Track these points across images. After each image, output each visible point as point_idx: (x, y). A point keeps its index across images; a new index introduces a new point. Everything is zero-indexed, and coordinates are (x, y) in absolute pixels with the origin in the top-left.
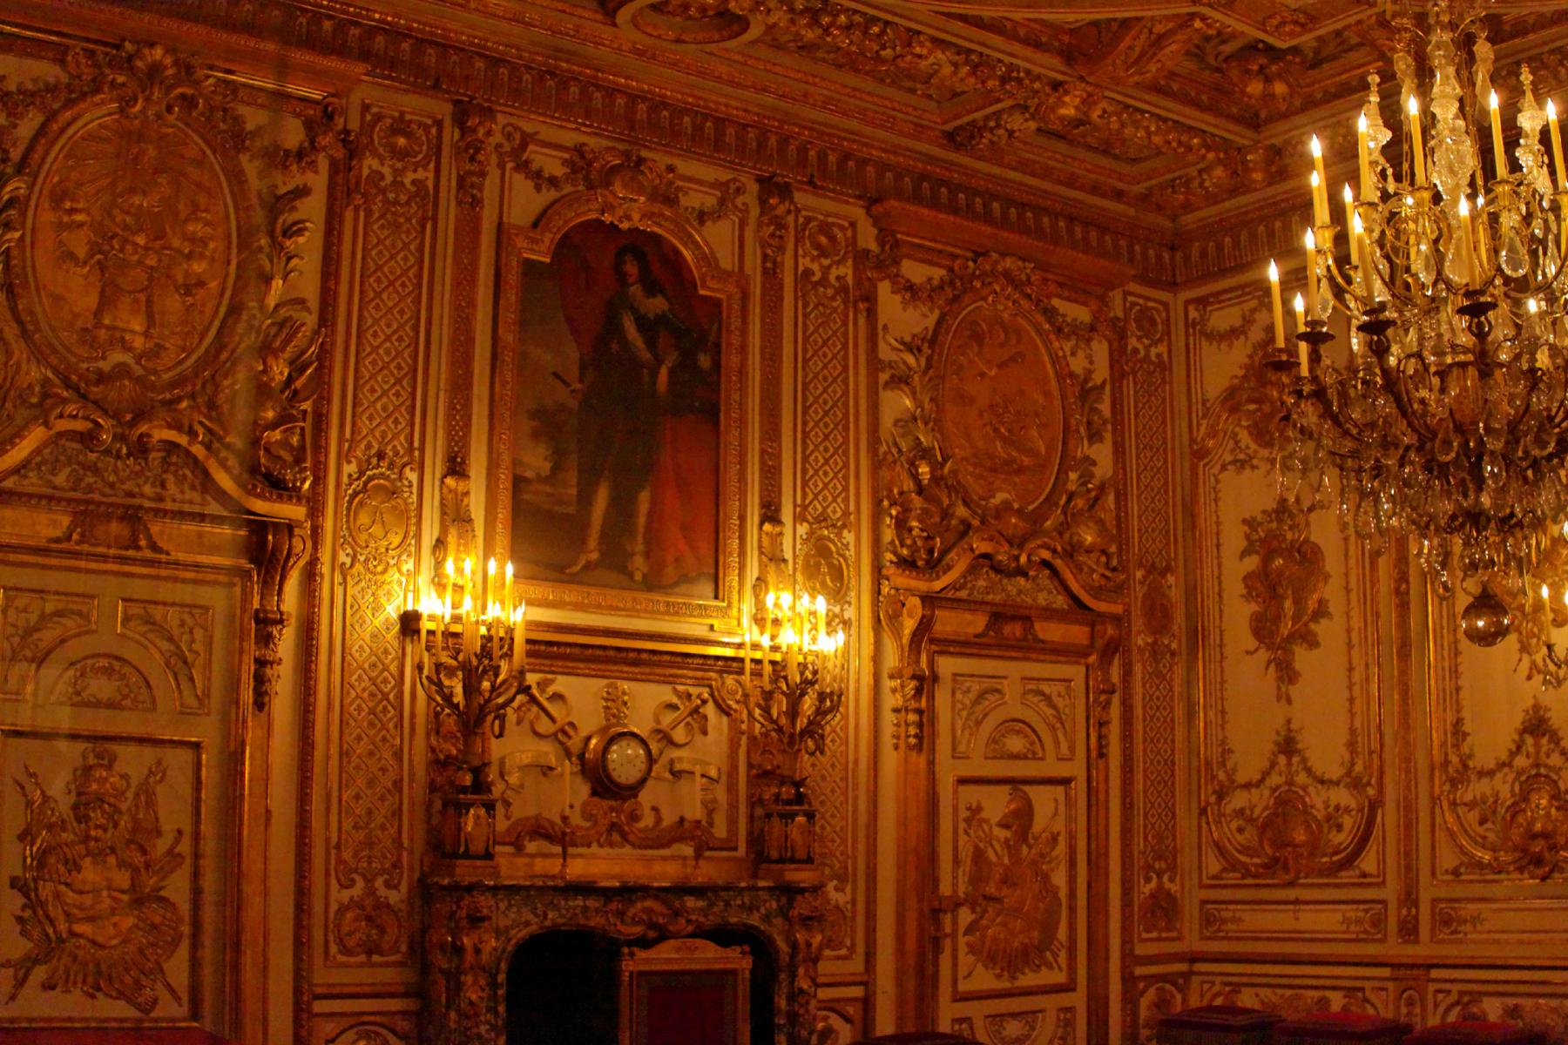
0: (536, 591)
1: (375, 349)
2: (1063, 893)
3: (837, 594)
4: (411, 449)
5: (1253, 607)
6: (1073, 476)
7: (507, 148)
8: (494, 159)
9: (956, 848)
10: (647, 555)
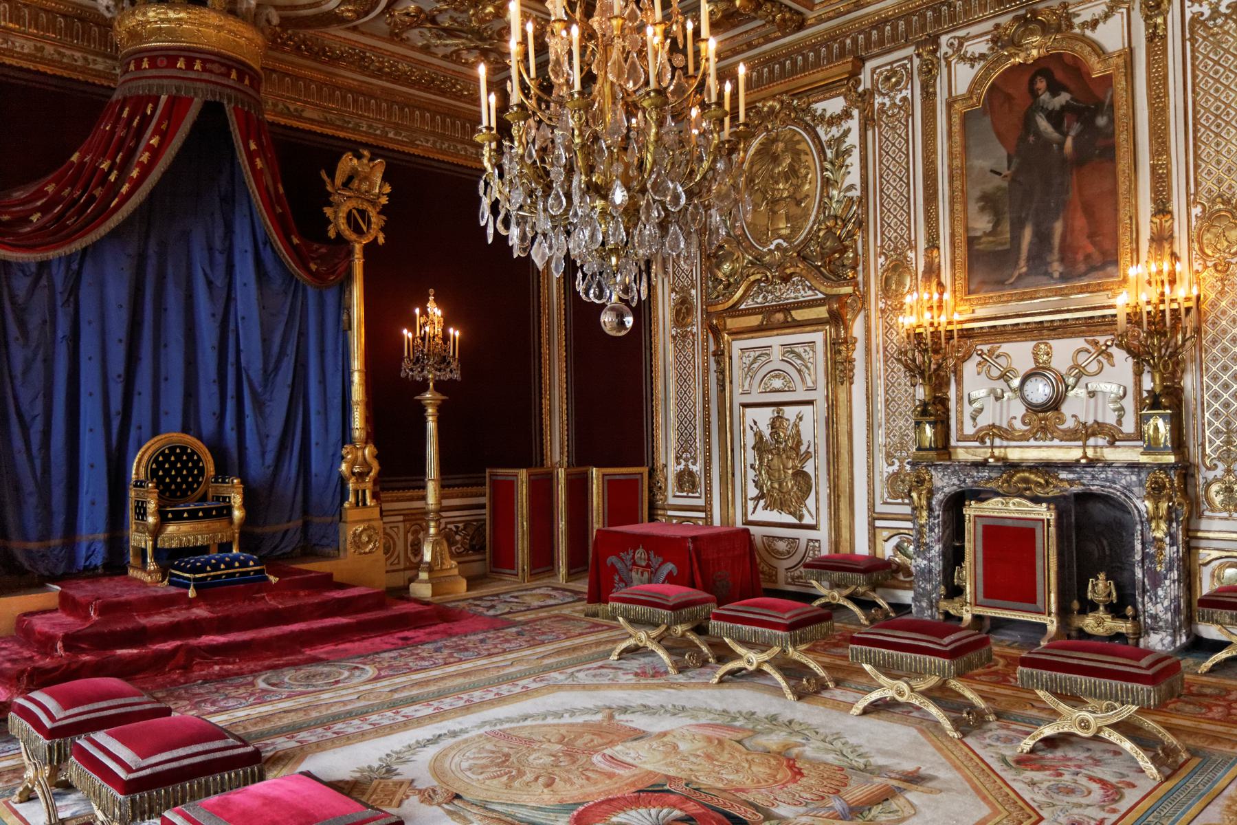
4: (909, 242)
10: (1062, 260)
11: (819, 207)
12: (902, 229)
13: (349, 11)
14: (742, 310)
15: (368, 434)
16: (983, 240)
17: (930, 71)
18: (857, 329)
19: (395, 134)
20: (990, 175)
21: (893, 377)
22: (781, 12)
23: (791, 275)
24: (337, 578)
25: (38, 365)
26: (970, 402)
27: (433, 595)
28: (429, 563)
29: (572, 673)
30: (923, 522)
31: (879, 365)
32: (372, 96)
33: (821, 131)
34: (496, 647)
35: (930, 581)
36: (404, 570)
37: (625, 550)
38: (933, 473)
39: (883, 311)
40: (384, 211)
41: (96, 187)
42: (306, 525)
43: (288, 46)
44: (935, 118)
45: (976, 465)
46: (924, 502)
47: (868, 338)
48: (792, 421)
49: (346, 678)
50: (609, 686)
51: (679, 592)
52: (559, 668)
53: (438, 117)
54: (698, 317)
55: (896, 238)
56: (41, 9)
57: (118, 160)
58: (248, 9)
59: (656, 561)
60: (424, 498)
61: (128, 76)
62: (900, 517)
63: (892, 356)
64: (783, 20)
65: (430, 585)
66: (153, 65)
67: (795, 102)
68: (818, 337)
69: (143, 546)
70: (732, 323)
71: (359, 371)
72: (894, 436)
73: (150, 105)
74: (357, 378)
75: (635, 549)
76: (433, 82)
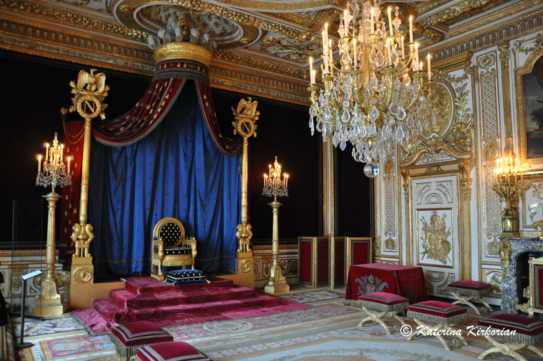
4: (497, 134)
11: (453, 119)
12: (493, 128)
13: (245, 41)
14: (417, 166)
15: (248, 220)
16: (534, 133)
17: (505, 56)
18: (472, 174)
19: (262, 91)
20: (537, 103)
21: (490, 197)
22: (433, 33)
23: (440, 150)
24: (234, 283)
25: (120, 188)
26: (530, 210)
27: (275, 292)
28: (273, 278)
29: (341, 332)
30: (507, 266)
31: (483, 191)
32: (252, 75)
33: (453, 84)
34: (305, 318)
35: (510, 295)
36: (262, 280)
37: (364, 276)
38: (512, 243)
39: (485, 166)
40: (257, 123)
41: (144, 116)
42: (221, 259)
43: (219, 56)
44: (508, 77)
45: (533, 240)
46: (507, 257)
48: (441, 217)
49: (240, 328)
50: (359, 339)
51: (391, 297)
52: (335, 329)
53: (280, 83)
54: (396, 169)
55: (491, 132)
56: (128, 48)
57: (153, 105)
58: (205, 42)
59: (378, 281)
60: (271, 249)
61: (158, 72)
62: (495, 263)
63: (490, 187)
64: (435, 36)
65: (273, 288)
66: (168, 66)
67: (441, 72)
68: (454, 178)
69: (157, 265)
70: (412, 172)
71: (245, 192)
72: (491, 225)
73: (166, 82)
74: (244, 195)
75: (369, 275)
76: (278, 68)
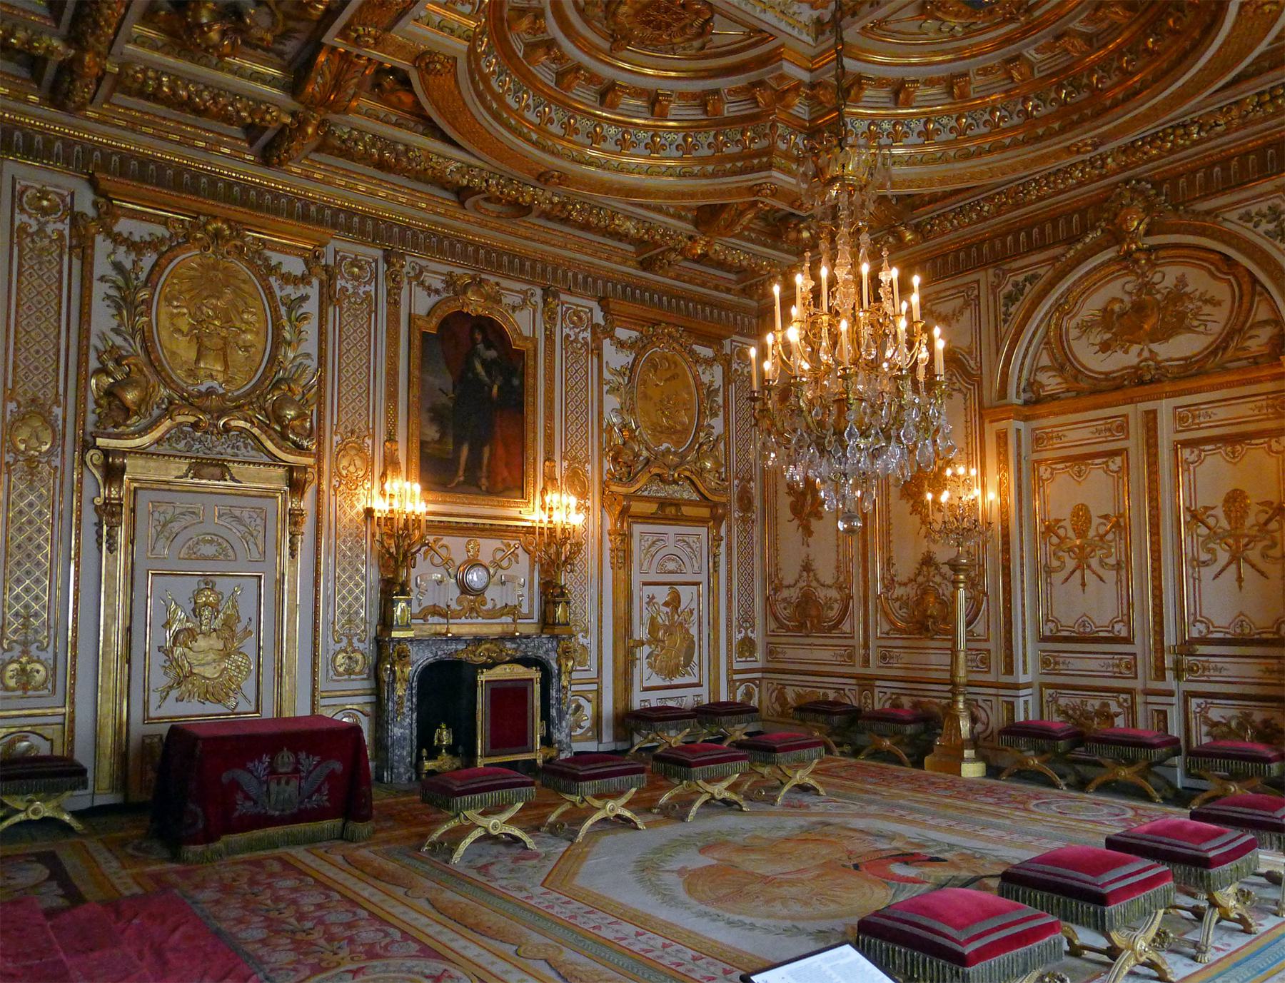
0: (430, 497)
1: (347, 379)
2: (696, 639)
3: (583, 495)
5: (792, 499)
6: (702, 434)
7: (412, 274)
8: (406, 280)
9: (641, 617)
10: (488, 478)
30: (400, 693)
39: (335, 490)
47: (318, 513)
